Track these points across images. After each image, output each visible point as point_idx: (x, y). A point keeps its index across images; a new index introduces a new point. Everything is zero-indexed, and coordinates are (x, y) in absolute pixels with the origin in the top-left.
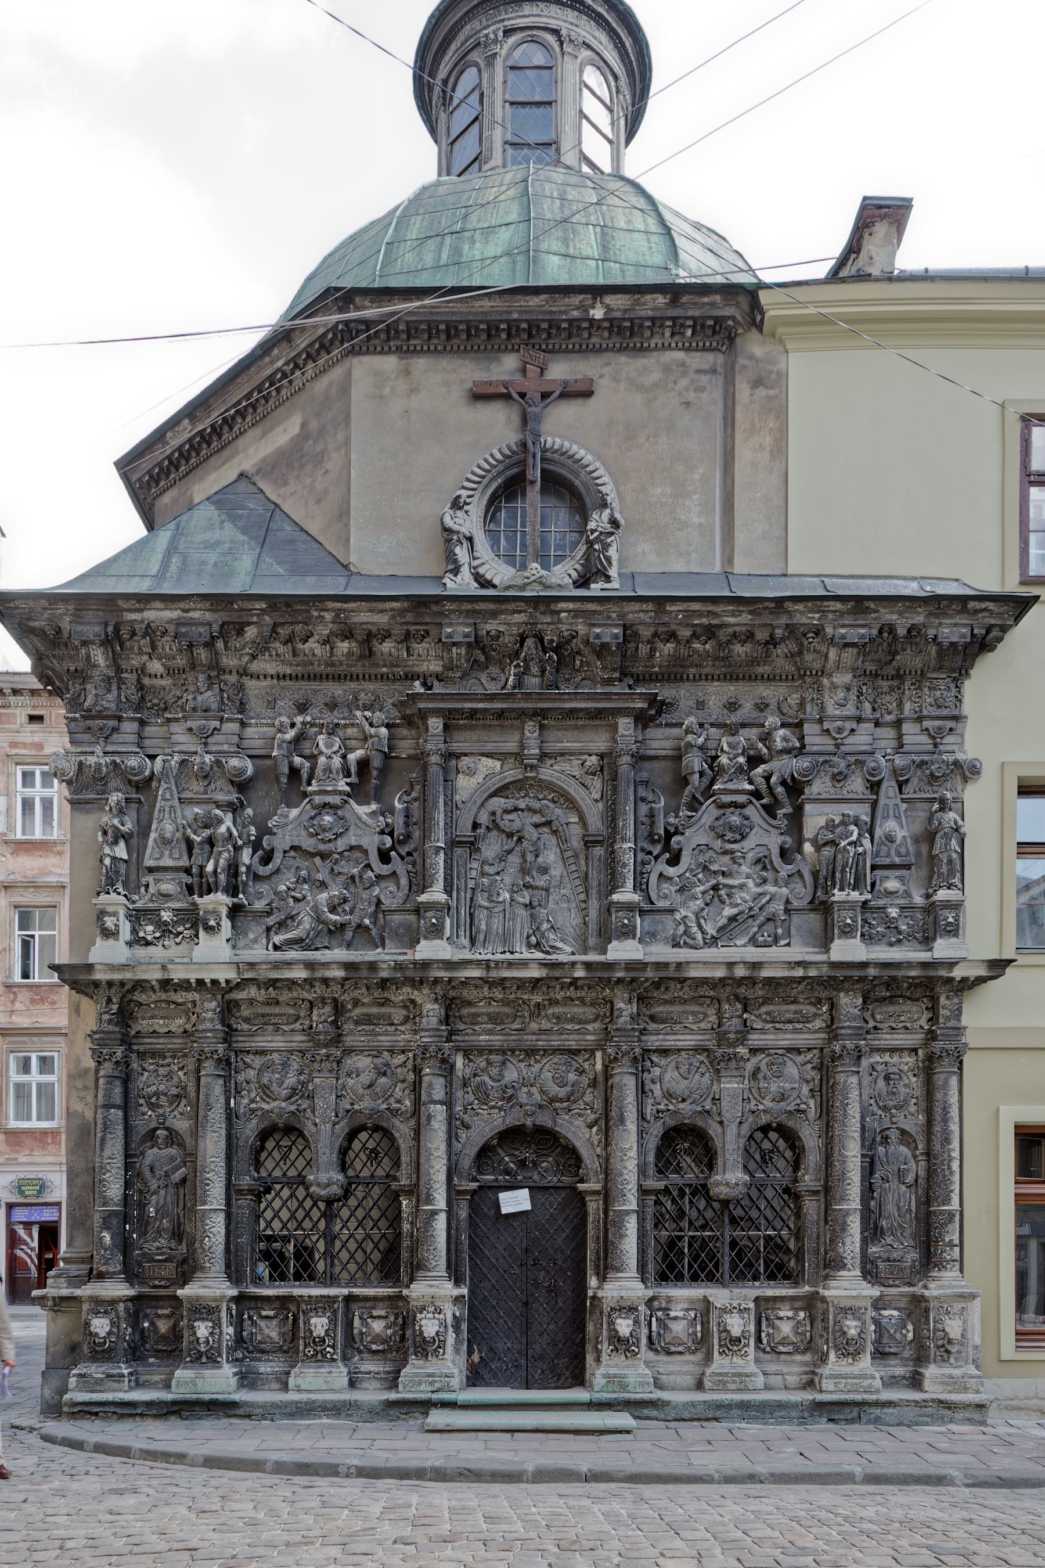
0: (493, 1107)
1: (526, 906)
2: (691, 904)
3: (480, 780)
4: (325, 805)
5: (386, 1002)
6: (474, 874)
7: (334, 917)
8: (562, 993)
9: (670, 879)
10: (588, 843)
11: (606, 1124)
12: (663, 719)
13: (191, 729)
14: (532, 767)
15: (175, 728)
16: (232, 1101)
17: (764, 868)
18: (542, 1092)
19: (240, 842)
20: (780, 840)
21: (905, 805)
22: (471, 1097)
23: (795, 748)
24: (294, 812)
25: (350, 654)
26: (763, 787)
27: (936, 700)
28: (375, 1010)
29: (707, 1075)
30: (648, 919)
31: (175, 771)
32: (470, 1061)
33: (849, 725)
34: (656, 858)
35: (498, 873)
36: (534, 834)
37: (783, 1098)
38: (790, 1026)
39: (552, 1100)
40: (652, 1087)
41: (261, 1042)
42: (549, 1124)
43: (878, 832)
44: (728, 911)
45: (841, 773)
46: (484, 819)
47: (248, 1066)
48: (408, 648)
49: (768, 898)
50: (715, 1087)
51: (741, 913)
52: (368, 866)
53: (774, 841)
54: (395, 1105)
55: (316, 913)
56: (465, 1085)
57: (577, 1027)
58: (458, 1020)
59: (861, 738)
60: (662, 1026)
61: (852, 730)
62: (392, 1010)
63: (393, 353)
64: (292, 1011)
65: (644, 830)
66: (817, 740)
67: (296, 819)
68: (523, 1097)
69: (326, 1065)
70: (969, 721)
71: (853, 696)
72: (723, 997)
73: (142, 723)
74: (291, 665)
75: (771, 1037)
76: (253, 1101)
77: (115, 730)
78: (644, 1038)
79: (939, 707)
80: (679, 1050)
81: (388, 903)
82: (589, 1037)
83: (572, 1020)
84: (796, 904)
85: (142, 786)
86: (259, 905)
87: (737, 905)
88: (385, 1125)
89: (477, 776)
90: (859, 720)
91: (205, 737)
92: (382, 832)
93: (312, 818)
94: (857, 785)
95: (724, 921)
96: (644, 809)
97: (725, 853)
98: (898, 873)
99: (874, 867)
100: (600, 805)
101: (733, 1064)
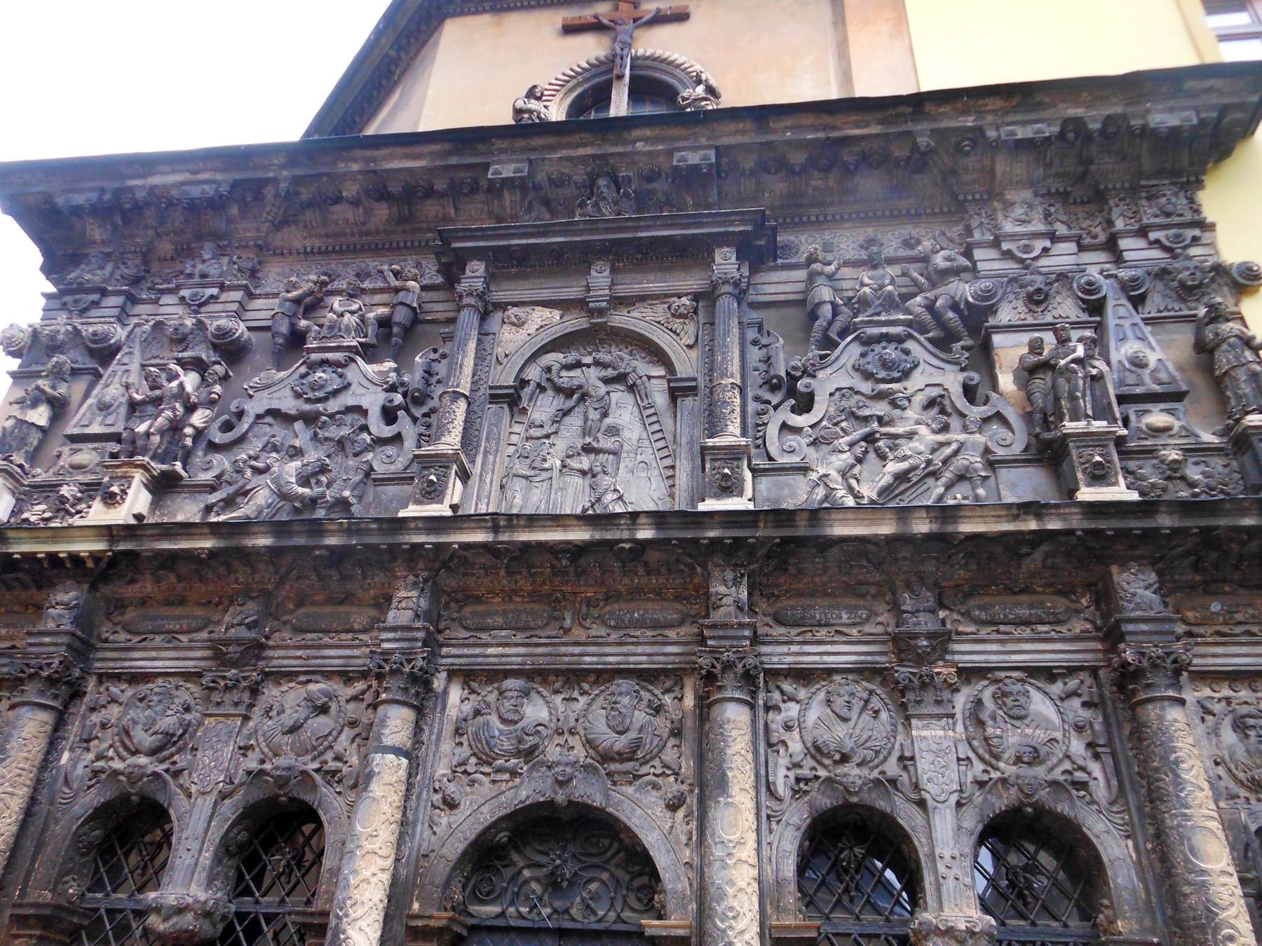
0: (499, 770)
1: (584, 473)
2: (833, 458)
3: (532, 331)
4: (324, 362)
5: (348, 599)
6: (514, 439)
7: (301, 490)
8: (626, 581)
9: (797, 430)
10: (677, 393)
11: (702, 800)
12: (779, 261)
13: (183, 298)
14: (601, 312)
15: (166, 299)
16: (66, 756)
17: (943, 411)
18: (589, 743)
19: (193, 399)
20: (961, 377)
21: (1149, 328)
22: (465, 751)
23: (965, 269)
24: (283, 374)
25: (388, 221)
26: (927, 317)
27: (1161, 209)
28: (327, 609)
29: (884, 715)
30: (765, 483)
31: (145, 336)
32: (473, 692)
33: (1039, 245)
34: (776, 408)
35: (548, 436)
36: (603, 389)
37: (1034, 757)
38: (1027, 632)
39: (606, 757)
40: (785, 736)
41: (141, 662)
42: (598, 800)
43: (1115, 356)
44: (893, 467)
45: (1039, 290)
46: (533, 373)
47: (113, 701)
48: (456, 209)
49: (954, 446)
50: (900, 738)
51: (914, 468)
52: (365, 428)
53: (953, 381)
54: (333, 765)
55: (279, 486)
56: (458, 732)
57: (649, 633)
58: (455, 625)
59: (1063, 257)
60: (794, 631)
61: (1045, 250)
62: (354, 609)
63: (488, 12)
64: (199, 612)
65: (755, 378)
66: (996, 265)
67: (282, 380)
68: (553, 752)
69: (235, 696)
70: (1218, 228)
71: (1038, 214)
72: (898, 583)
73: (133, 300)
74: (319, 236)
75: (994, 647)
76: (100, 757)
77: (95, 304)
78: (764, 649)
79: (1168, 215)
80: (828, 673)
81: (380, 469)
82: (670, 649)
83: (641, 624)
84: (1001, 452)
85: (104, 353)
86: (206, 477)
87: (905, 458)
88: (308, 798)
89: (528, 327)
90: (1054, 238)
91: (196, 306)
92: (392, 388)
93: (303, 376)
94: (1066, 308)
95: (886, 480)
96: (755, 354)
97: (879, 396)
98: (1162, 406)
99: (1122, 399)
100: (694, 354)
101: (929, 696)
